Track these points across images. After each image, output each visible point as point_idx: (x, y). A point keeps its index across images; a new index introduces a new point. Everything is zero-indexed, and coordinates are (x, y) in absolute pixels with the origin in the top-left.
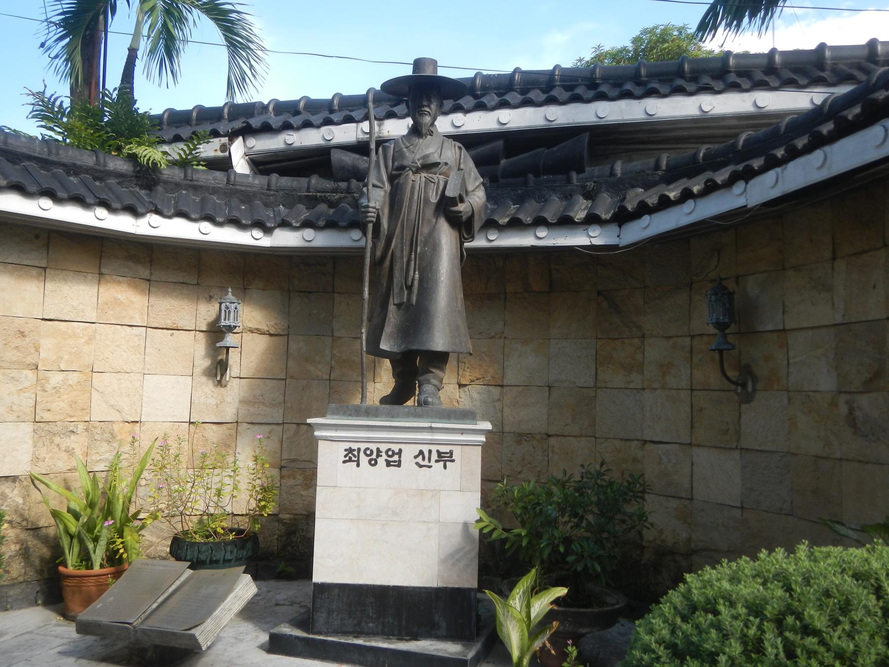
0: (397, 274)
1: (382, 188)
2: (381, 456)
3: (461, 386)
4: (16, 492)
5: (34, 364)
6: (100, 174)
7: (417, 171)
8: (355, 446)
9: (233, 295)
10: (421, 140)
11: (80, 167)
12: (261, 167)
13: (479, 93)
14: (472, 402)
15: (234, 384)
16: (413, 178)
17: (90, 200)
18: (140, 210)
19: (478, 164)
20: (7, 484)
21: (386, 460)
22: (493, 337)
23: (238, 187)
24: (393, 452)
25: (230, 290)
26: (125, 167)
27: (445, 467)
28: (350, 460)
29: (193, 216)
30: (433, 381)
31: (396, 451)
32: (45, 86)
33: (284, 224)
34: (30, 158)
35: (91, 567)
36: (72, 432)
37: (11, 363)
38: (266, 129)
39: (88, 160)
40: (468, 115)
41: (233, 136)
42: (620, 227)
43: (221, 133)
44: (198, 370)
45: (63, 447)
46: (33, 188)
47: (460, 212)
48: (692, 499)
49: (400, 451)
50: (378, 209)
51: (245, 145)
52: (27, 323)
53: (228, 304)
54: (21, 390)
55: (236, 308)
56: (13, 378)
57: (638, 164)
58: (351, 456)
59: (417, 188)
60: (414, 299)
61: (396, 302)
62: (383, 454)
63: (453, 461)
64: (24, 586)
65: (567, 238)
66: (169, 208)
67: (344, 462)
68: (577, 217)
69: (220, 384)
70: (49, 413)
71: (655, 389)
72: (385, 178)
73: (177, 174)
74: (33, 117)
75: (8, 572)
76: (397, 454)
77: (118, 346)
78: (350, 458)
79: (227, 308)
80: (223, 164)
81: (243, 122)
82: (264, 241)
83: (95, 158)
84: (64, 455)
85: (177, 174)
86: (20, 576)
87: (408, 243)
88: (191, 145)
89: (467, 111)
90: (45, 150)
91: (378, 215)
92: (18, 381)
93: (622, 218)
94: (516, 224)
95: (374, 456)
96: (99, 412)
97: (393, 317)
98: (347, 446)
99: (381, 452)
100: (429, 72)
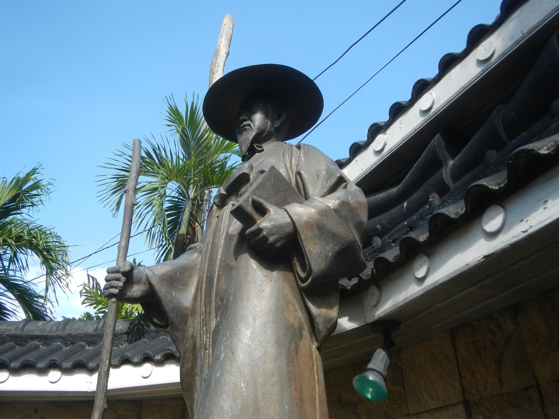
11: (75, 336)
40: (388, 131)
65: (550, 204)
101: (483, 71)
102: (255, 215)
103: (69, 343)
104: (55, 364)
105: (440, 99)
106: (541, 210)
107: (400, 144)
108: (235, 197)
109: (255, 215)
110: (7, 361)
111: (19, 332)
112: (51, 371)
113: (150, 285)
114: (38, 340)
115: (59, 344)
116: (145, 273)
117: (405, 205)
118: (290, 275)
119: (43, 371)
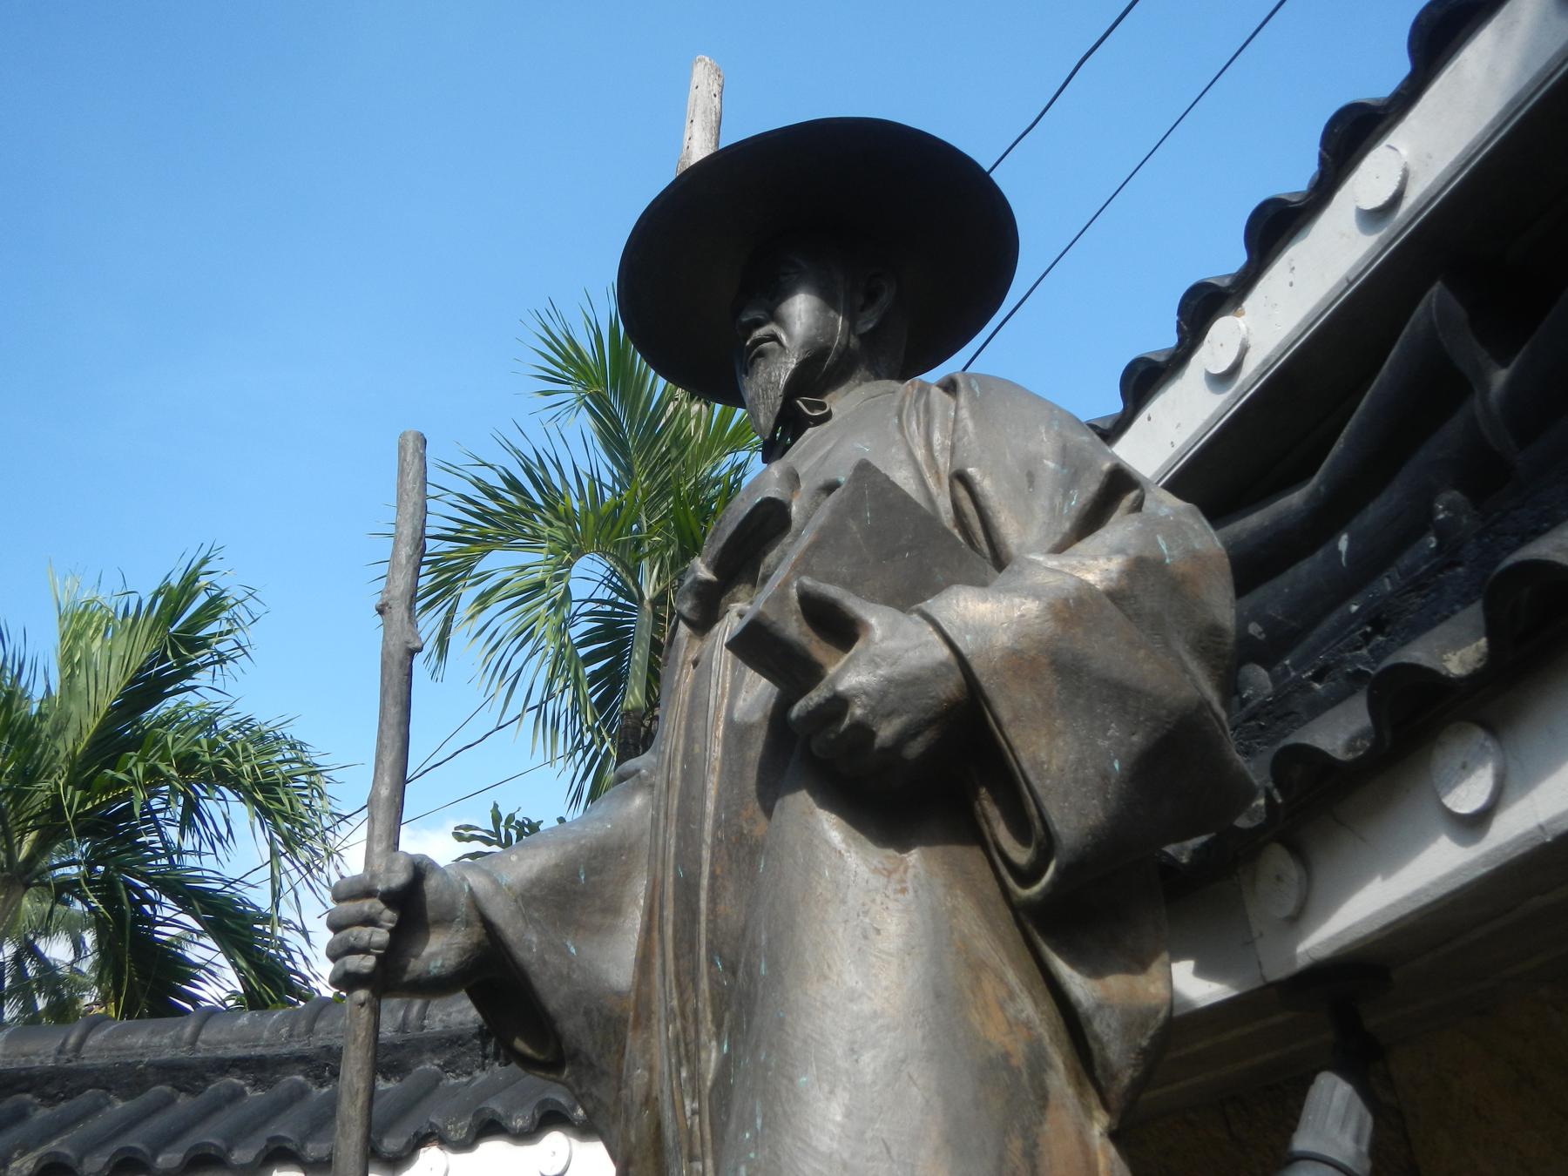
40: (1248, 304)
102: (818, 649)
103: (327, 1074)
104: (285, 1149)
105: (1431, 157)
107: (1299, 338)
108: (748, 586)
109: (818, 649)
110: (145, 1150)
111: (182, 1054)
112: (275, 1172)
113: (488, 925)
114: (239, 1073)
115: (297, 1082)
116: (466, 887)
117: (1343, 543)
118: (971, 857)
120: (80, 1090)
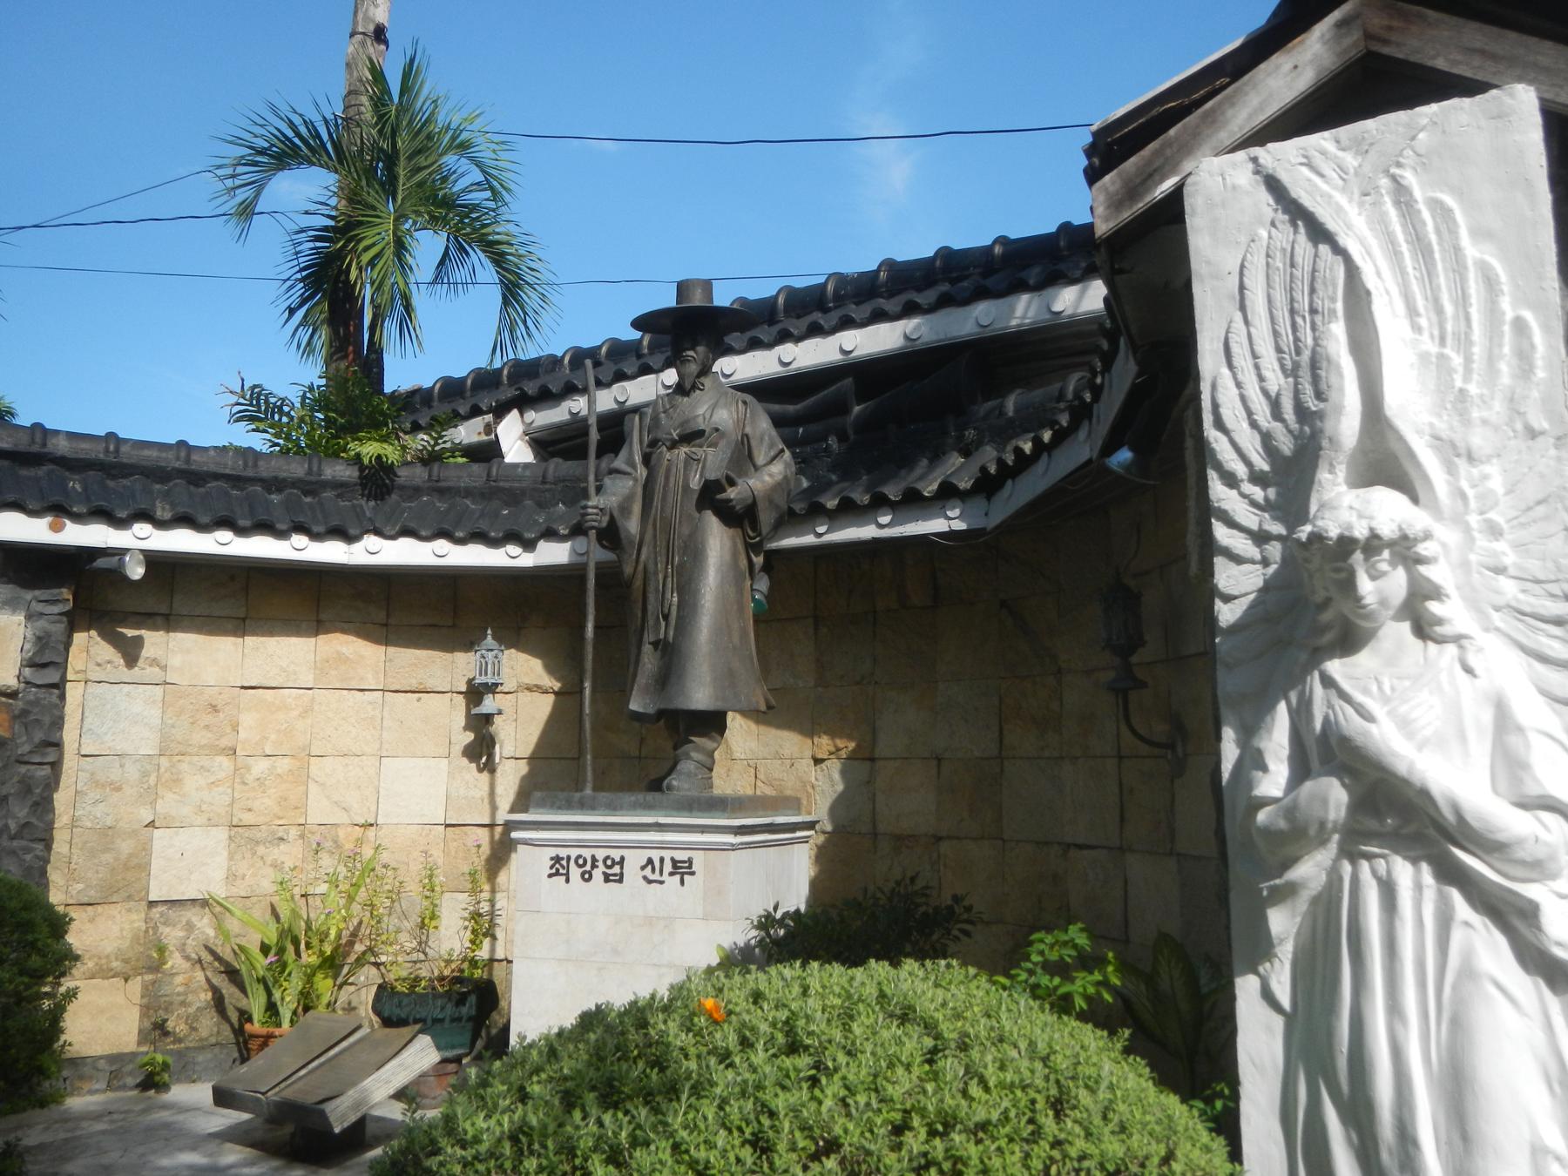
0: (651, 598)
1: (625, 473)
2: (597, 867)
3: (817, 761)
4: (206, 920)
5: (230, 749)
6: (311, 487)
7: (674, 445)
8: (563, 853)
9: (494, 638)
10: (686, 399)
11: (284, 480)
12: (551, 449)
13: (831, 305)
14: (833, 786)
15: (506, 768)
16: (668, 456)
17: (281, 526)
18: (352, 532)
19: (778, 422)
20: (194, 910)
21: (604, 873)
22: (858, 683)
23: (501, 484)
24: (613, 860)
25: (489, 632)
26: (348, 473)
27: (682, 882)
28: (557, 873)
29: (423, 533)
30: (694, 755)
31: (617, 859)
32: (243, 380)
33: (550, 534)
34: (217, 476)
35: (279, 1025)
36: (282, 839)
37: (201, 747)
38: (546, 397)
39: (296, 469)
41: (500, 412)
42: (989, 499)
43: (484, 409)
44: (458, 749)
45: (269, 860)
46: (205, 519)
47: (731, 500)
48: (1127, 941)
49: (622, 859)
50: (601, 510)
51: (523, 421)
52: (220, 694)
53: (484, 652)
54: (213, 783)
55: (496, 657)
56: (202, 767)
57: (1037, 395)
58: (559, 868)
59: (674, 470)
60: (671, 633)
61: (652, 640)
62: (600, 864)
63: (693, 873)
64: (217, 1050)
66: (394, 526)
67: (550, 876)
68: (930, 488)
69: (490, 768)
70: (250, 813)
71: (1077, 758)
72: (638, 458)
73: (419, 474)
74: (235, 421)
75: (194, 1029)
76: (618, 863)
77: (344, 719)
78: (558, 870)
79: (483, 657)
80: (488, 452)
81: (516, 390)
82: (526, 560)
83: (306, 466)
84: (270, 871)
85: (419, 474)
86: (212, 1035)
87: (664, 551)
88: (433, 434)
89: (798, 339)
90: (240, 463)
91: (612, 518)
92: (209, 771)
93: (987, 486)
94: (848, 511)
95: (588, 868)
96: (319, 811)
97: (649, 660)
98: (553, 852)
99: (597, 861)
100: (697, 300)
101: (906, 347)
102: (727, 486)
106: (913, 524)
109: (727, 486)
117: (801, 430)
118: (739, 530)
119: (281, 535)
120: (132, 475)
